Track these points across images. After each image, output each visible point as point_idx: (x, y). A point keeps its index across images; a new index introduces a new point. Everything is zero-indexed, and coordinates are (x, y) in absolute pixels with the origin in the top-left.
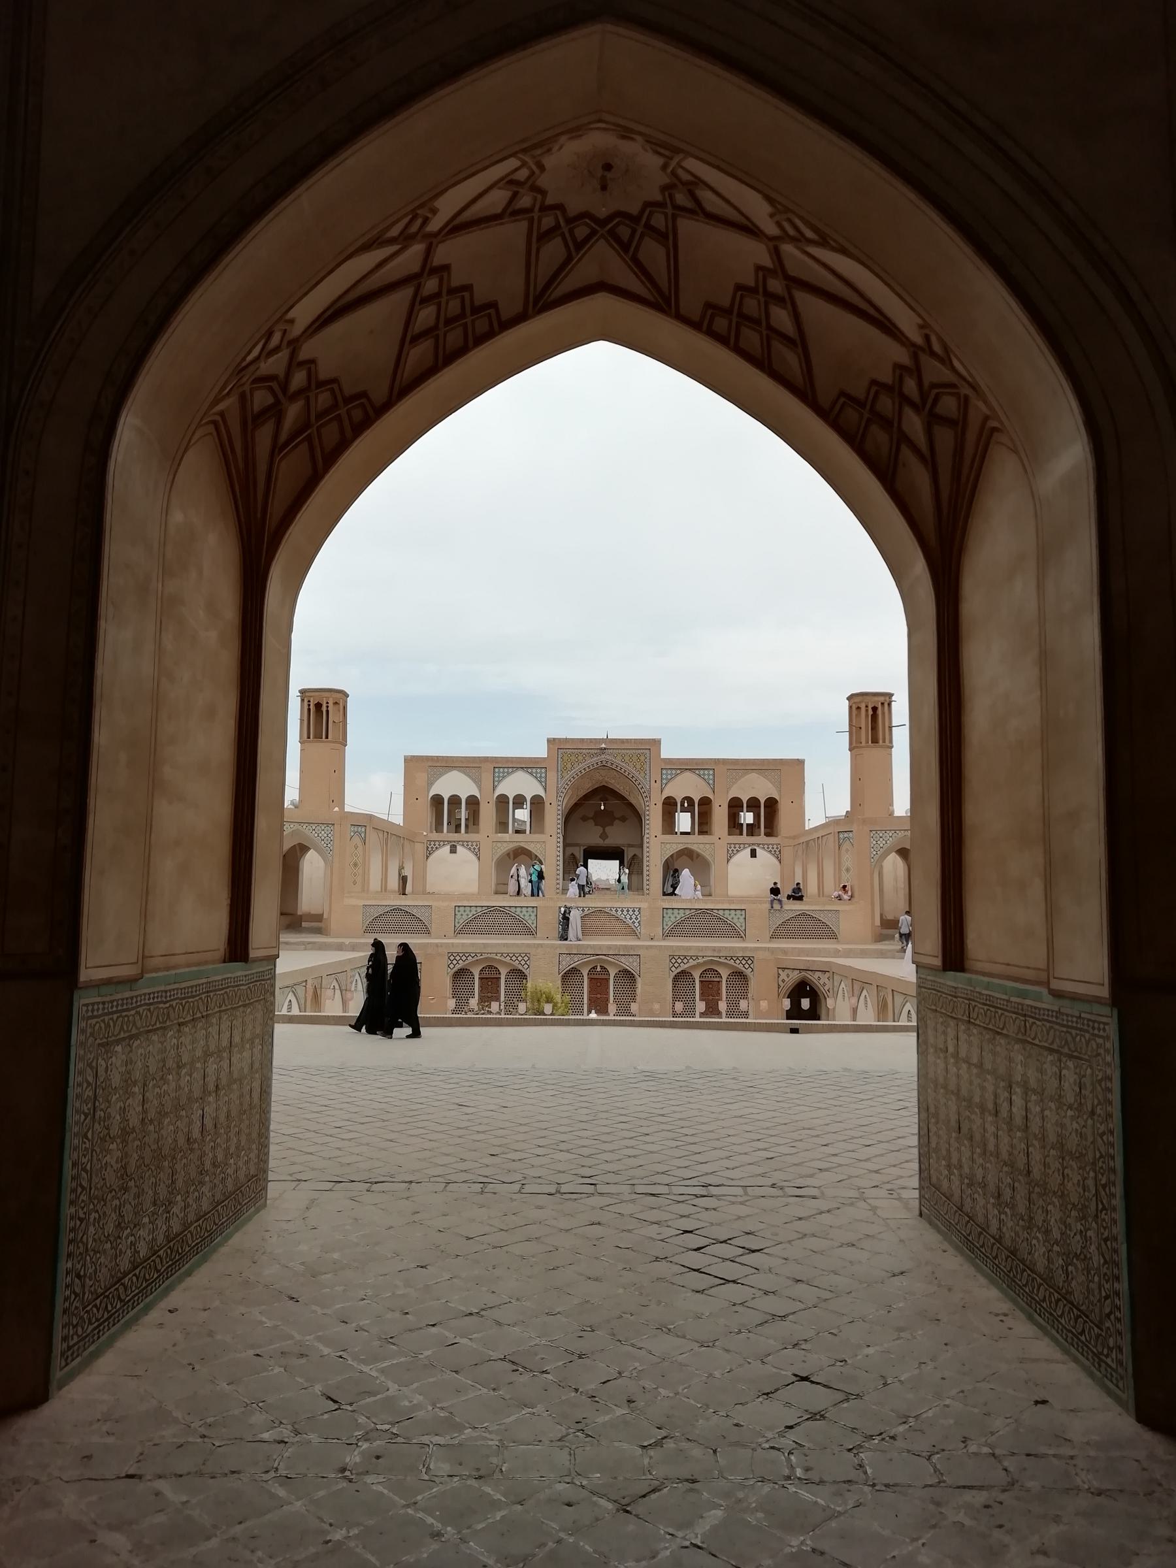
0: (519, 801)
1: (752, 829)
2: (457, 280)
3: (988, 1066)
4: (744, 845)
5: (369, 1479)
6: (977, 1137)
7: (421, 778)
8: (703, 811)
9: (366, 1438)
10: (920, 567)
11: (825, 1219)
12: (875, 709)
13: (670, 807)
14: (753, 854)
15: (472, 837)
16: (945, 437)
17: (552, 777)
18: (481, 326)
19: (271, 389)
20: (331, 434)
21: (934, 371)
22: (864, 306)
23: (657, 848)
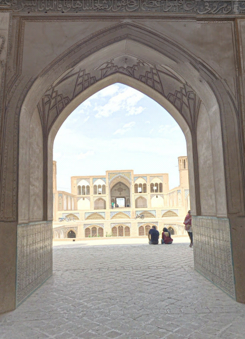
0: (99, 186)
1: (156, 191)
2: (87, 72)
3: (206, 235)
4: (154, 195)
5: (84, 318)
6: (205, 250)
7: (75, 182)
8: (144, 187)
9: (82, 312)
10: (188, 129)
11: (175, 272)
12: (184, 160)
13: (136, 186)
14: (157, 197)
15: (88, 196)
16: (191, 102)
17: (107, 180)
18: (92, 81)
19: (49, 97)
20: (61, 106)
21: (188, 89)
22: (173, 75)
23: (133, 197)
